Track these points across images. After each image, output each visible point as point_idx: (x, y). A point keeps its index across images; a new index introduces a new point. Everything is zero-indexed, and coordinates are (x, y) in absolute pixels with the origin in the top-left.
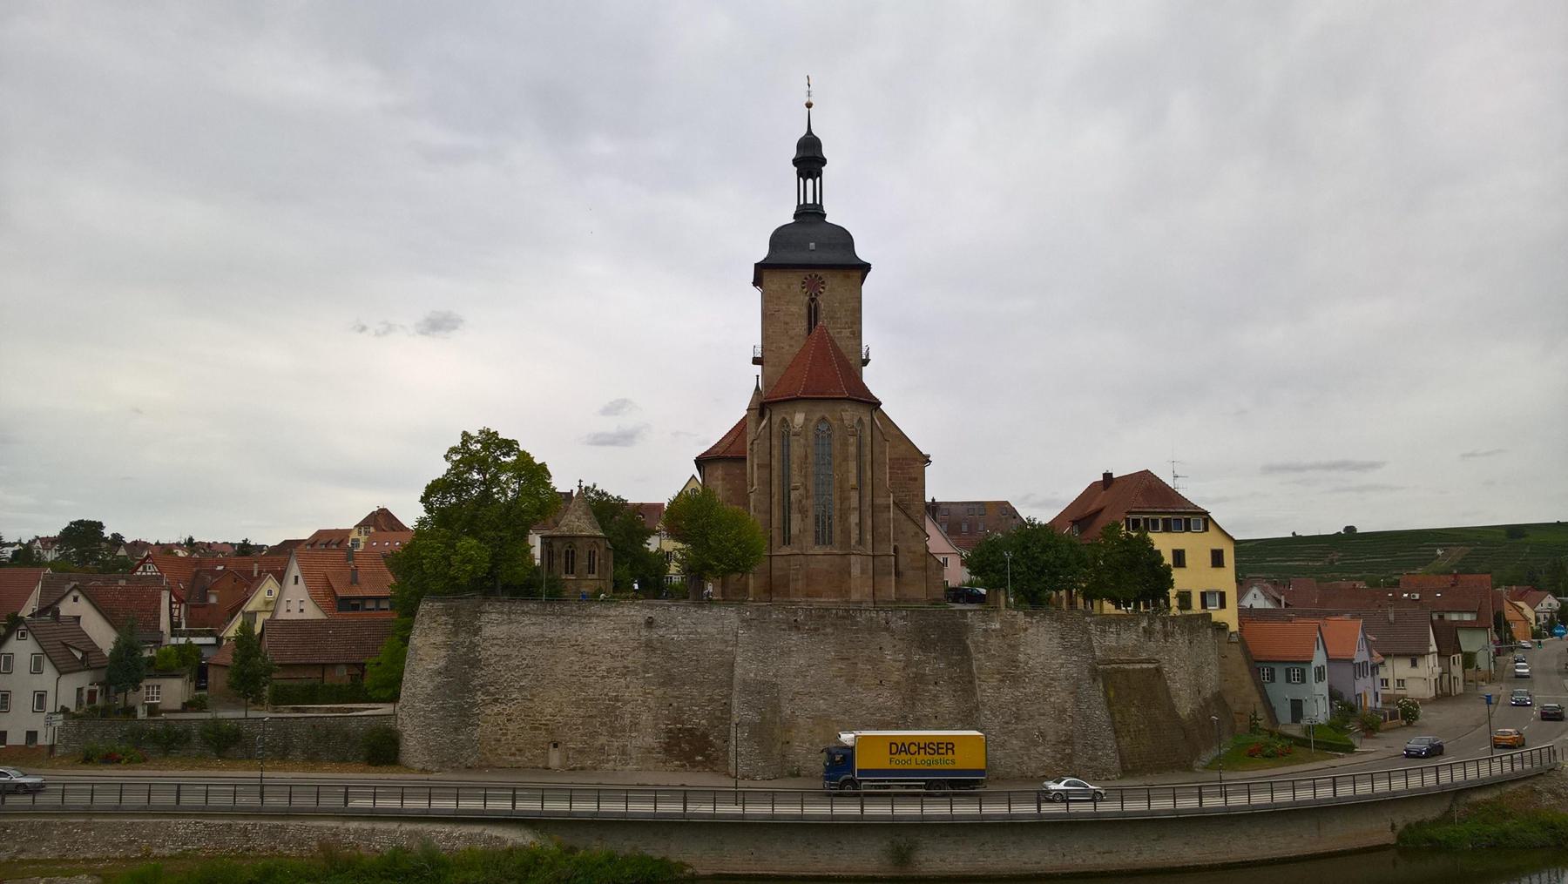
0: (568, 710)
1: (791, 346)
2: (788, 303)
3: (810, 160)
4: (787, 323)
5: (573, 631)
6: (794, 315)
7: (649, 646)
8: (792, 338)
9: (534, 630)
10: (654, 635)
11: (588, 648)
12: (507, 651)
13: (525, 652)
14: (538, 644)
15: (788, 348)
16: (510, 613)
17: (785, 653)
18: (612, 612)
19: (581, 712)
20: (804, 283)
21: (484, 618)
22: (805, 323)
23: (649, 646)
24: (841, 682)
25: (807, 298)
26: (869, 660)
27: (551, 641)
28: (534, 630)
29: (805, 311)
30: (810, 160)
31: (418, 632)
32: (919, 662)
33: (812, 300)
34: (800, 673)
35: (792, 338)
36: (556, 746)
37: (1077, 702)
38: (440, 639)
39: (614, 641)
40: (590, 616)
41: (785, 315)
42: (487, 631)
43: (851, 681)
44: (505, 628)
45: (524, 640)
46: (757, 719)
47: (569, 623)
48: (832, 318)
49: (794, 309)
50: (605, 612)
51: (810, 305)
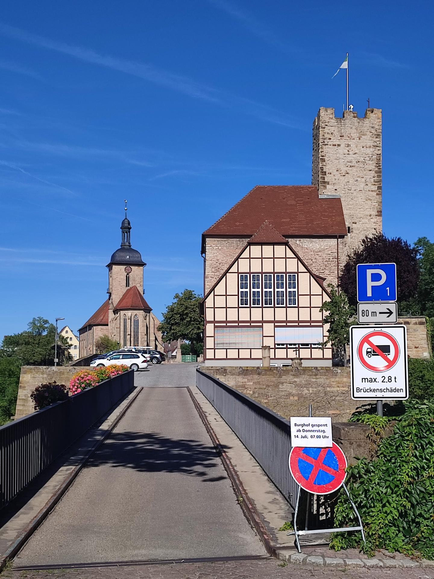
1: (121, 289)
2: (120, 275)
3: (126, 228)
4: (120, 282)
6: (122, 279)
8: (121, 286)
15: (120, 289)
20: (125, 269)
22: (125, 282)
25: (126, 274)
29: (125, 278)
30: (126, 228)
33: (128, 274)
35: (121, 286)
41: (119, 279)
48: (134, 280)
49: (122, 277)
51: (127, 276)
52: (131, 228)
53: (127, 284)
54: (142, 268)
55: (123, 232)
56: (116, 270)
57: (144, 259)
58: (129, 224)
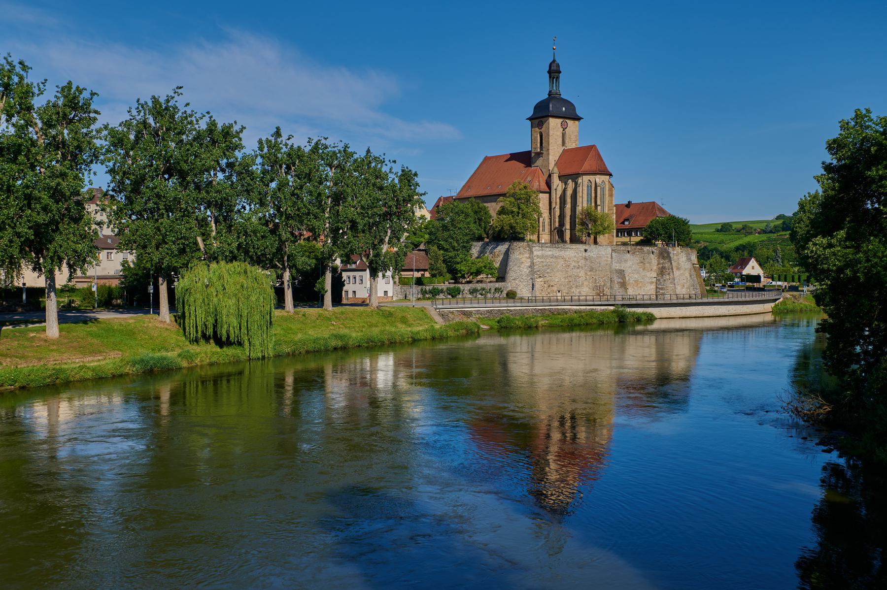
0: (563, 280)
3: (554, 72)
5: (562, 253)
7: (586, 259)
9: (550, 253)
10: (587, 254)
11: (567, 259)
12: (542, 260)
13: (548, 260)
14: (552, 258)
16: (542, 247)
17: (626, 261)
18: (574, 247)
19: (567, 280)
21: (534, 249)
23: (586, 259)
24: (641, 269)
26: (649, 263)
27: (555, 257)
28: (550, 253)
30: (554, 72)
31: (518, 253)
32: (663, 263)
34: (630, 267)
36: (559, 292)
37: (691, 276)
38: (528, 255)
39: (575, 256)
40: (567, 248)
42: (535, 253)
43: (644, 269)
44: (540, 252)
45: (546, 256)
46: (622, 281)
47: (561, 251)
50: (572, 247)
52: (560, 72)
53: (564, 143)
54: (577, 122)
55: (550, 77)
56: (552, 124)
57: (579, 113)
58: (558, 66)
